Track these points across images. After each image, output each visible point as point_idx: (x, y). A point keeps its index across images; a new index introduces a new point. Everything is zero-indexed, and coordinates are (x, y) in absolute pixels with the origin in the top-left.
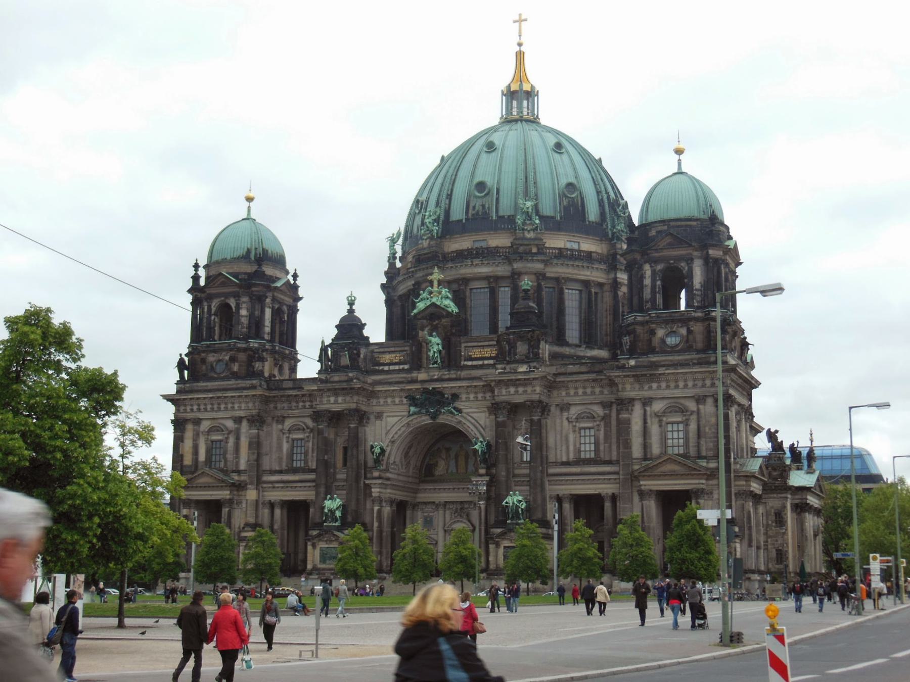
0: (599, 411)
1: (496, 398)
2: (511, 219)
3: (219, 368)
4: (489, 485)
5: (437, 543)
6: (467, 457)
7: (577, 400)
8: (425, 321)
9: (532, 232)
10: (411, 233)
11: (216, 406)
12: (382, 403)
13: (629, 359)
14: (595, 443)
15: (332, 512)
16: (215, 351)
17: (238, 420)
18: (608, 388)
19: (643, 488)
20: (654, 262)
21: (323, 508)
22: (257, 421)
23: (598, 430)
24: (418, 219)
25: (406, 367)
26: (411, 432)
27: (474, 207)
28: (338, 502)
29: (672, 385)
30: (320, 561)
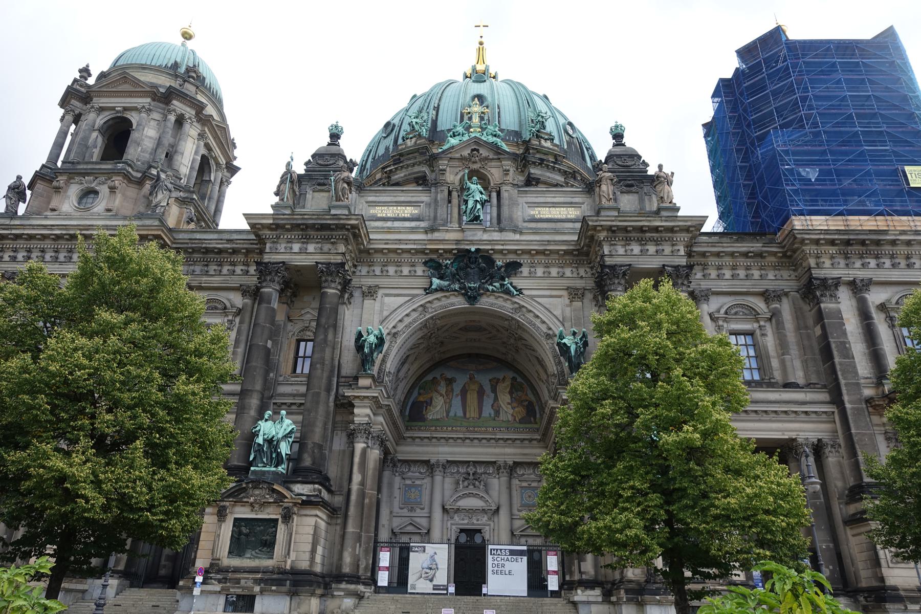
0: (760, 305)
1: (606, 259)
2: (517, 134)
5: (429, 531)
6: (481, 393)
7: (723, 286)
9: (549, 142)
10: (374, 159)
11: (62, 256)
12: (378, 272)
14: (757, 357)
15: (272, 443)
18: (777, 272)
21: (256, 435)
23: (763, 335)
25: (423, 224)
26: (425, 325)
29: (903, 263)
30: (230, 552)
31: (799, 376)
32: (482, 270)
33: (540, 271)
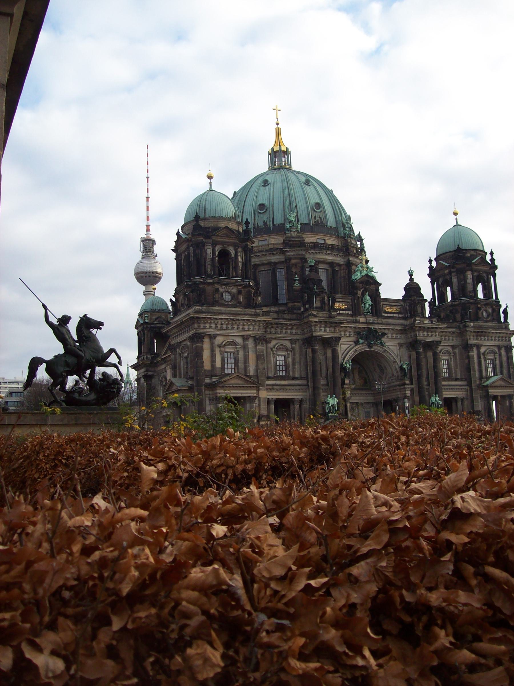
0: (450, 349)
2: (336, 229)
3: (227, 297)
4: (412, 390)
8: (361, 285)
10: (254, 225)
11: (230, 327)
13: (471, 322)
16: (227, 284)
17: (245, 338)
19: (490, 393)
20: (473, 271)
21: (329, 403)
22: (257, 340)
24: (265, 217)
25: (350, 313)
27: (315, 218)
28: (336, 401)
31: (459, 377)
32: (374, 336)
33: (390, 335)
